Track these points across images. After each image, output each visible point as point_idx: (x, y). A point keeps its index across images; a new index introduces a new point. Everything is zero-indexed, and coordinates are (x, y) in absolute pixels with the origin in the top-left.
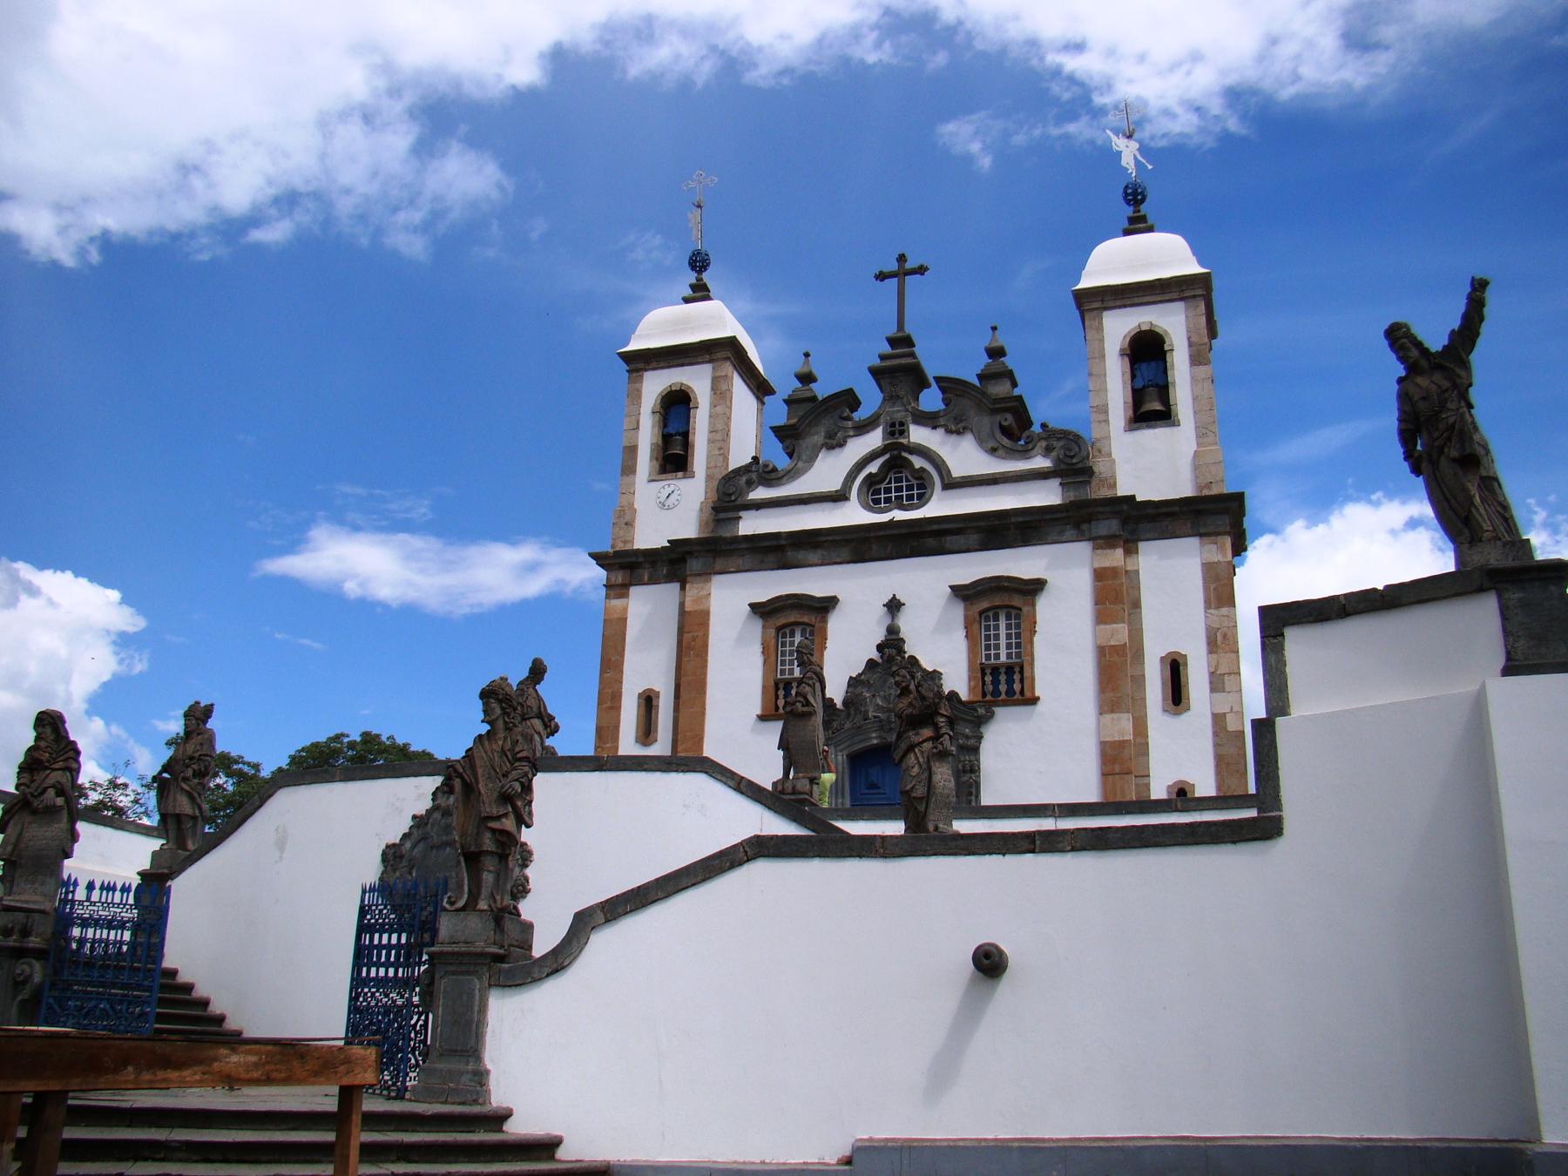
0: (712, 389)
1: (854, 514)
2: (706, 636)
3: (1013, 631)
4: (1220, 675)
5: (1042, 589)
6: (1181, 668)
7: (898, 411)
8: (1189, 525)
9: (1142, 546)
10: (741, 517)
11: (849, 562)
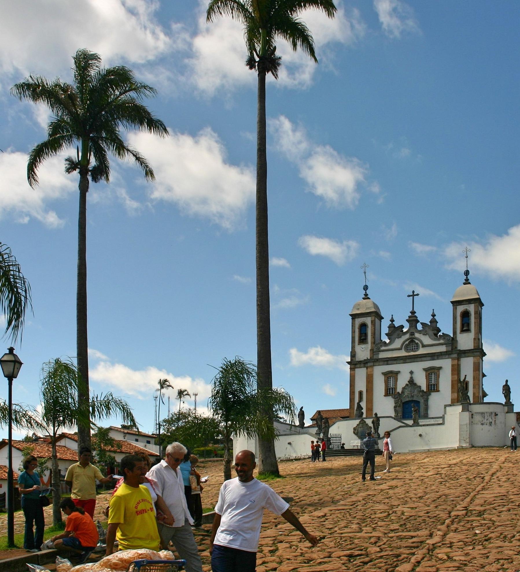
1: (403, 353)
2: (373, 379)
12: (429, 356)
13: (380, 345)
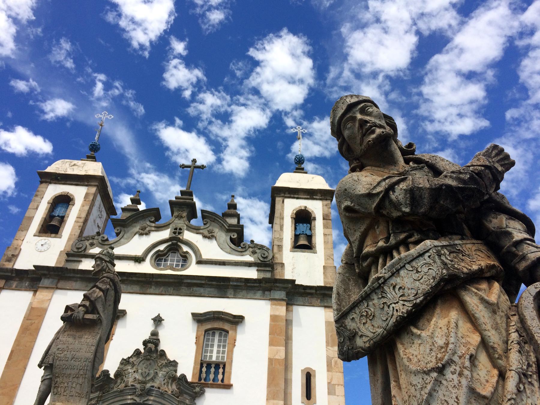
0: (84, 198)
3: (222, 344)
4: (333, 384)
5: (241, 322)
6: (312, 378)
7: (180, 223)
8: (319, 301)
9: (295, 308)
10: (81, 261)
11: (137, 293)
12: (211, 286)
13: (91, 241)
